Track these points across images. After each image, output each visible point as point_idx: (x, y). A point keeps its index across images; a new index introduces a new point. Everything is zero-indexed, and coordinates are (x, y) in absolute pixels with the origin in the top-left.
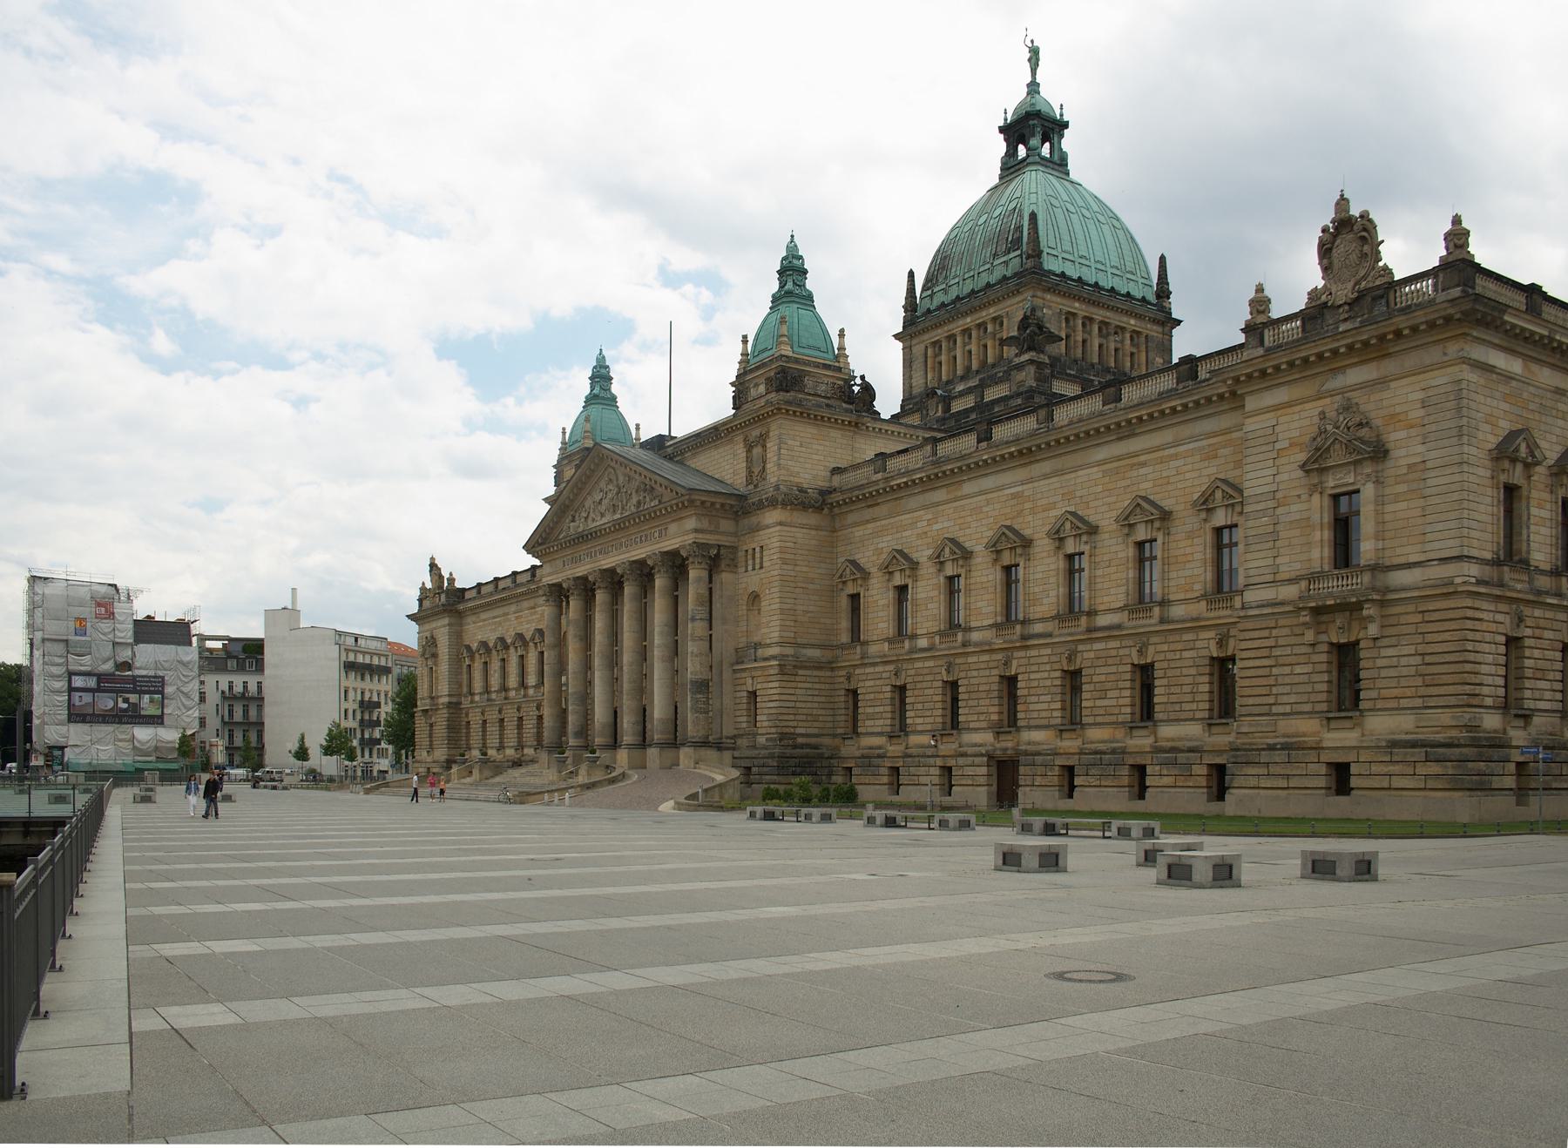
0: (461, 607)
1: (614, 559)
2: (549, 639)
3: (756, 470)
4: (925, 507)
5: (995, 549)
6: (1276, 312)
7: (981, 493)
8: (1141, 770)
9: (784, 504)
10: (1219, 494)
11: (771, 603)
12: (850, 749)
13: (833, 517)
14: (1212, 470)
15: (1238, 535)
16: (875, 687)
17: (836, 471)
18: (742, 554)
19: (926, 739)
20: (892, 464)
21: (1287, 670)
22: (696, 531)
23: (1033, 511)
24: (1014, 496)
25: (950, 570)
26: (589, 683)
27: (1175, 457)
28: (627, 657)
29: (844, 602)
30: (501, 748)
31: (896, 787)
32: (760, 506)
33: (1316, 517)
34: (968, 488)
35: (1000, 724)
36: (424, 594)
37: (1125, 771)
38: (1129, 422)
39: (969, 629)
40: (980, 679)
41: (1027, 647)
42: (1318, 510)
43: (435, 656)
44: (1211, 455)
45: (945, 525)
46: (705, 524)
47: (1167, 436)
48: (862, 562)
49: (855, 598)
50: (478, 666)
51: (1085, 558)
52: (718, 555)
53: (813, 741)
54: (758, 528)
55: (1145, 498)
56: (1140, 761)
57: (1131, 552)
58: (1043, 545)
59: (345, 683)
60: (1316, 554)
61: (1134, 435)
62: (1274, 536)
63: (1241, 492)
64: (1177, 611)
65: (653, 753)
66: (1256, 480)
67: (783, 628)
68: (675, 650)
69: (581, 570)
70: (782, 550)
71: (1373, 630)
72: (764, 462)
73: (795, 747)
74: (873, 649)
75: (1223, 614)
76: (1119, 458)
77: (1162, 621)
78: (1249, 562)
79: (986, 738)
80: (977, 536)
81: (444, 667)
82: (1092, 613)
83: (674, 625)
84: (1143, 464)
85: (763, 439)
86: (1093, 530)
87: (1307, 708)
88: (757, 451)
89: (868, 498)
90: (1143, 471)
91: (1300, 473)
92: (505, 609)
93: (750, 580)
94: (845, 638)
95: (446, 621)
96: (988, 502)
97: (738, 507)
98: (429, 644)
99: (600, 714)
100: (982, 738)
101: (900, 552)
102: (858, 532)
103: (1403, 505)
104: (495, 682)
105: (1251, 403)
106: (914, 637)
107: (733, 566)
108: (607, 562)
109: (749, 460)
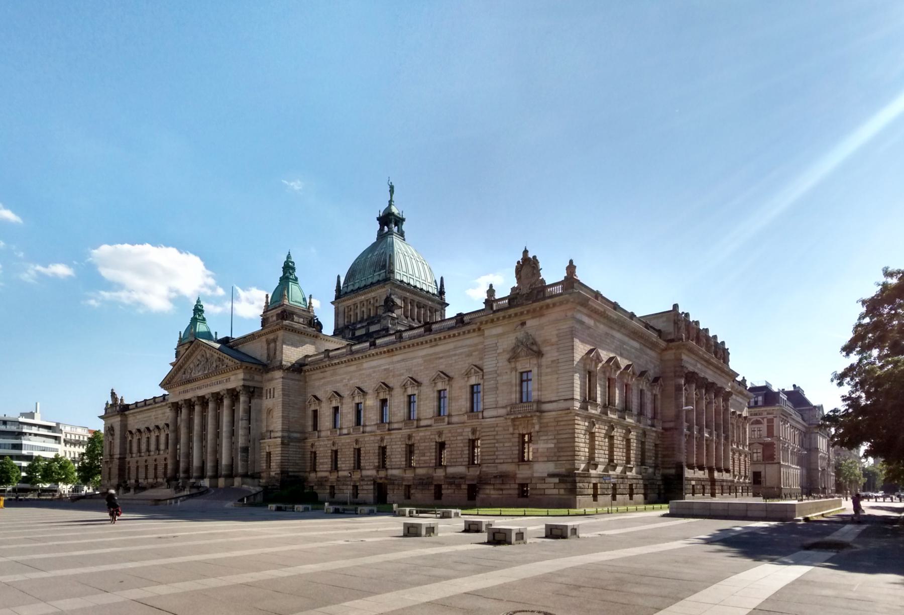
3: (272, 354)
4: (346, 373)
5: (377, 391)
6: (497, 296)
7: (372, 368)
8: (439, 488)
10: (473, 371)
14: (471, 360)
15: (481, 388)
18: (264, 391)
19: (346, 473)
21: (501, 445)
22: (244, 380)
23: (394, 376)
24: (385, 370)
25: (357, 400)
26: (190, 448)
27: (455, 355)
28: (210, 436)
29: (310, 413)
32: (273, 369)
33: (514, 382)
34: (365, 365)
35: (379, 467)
37: (432, 487)
38: (435, 340)
39: (365, 426)
41: (390, 434)
42: (514, 378)
44: (469, 355)
45: (356, 382)
46: (248, 377)
47: (451, 346)
48: (319, 396)
49: (315, 412)
51: (416, 397)
52: (253, 392)
54: (272, 379)
55: (442, 372)
56: (439, 483)
57: (436, 394)
58: (397, 391)
60: (513, 396)
61: (437, 345)
62: (497, 388)
63: (482, 370)
64: (454, 419)
66: (489, 365)
68: (232, 433)
70: (283, 390)
71: (537, 428)
72: (275, 350)
74: (323, 434)
75: (475, 422)
76: (431, 355)
77: (449, 423)
78: (487, 400)
79: (372, 473)
80: (369, 386)
82: (419, 420)
83: (232, 422)
84: (441, 358)
85: (275, 340)
86: (419, 384)
87: (510, 460)
88: (272, 345)
90: (441, 361)
91: (507, 363)
93: (267, 403)
94: (310, 429)
96: (374, 372)
99: (196, 462)
100: (371, 473)
101: (336, 392)
102: (317, 383)
103: (549, 377)
105: (487, 333)
106: (341, 429)
107: (260, 396)
108: (201, 393)
109: (268, 349)
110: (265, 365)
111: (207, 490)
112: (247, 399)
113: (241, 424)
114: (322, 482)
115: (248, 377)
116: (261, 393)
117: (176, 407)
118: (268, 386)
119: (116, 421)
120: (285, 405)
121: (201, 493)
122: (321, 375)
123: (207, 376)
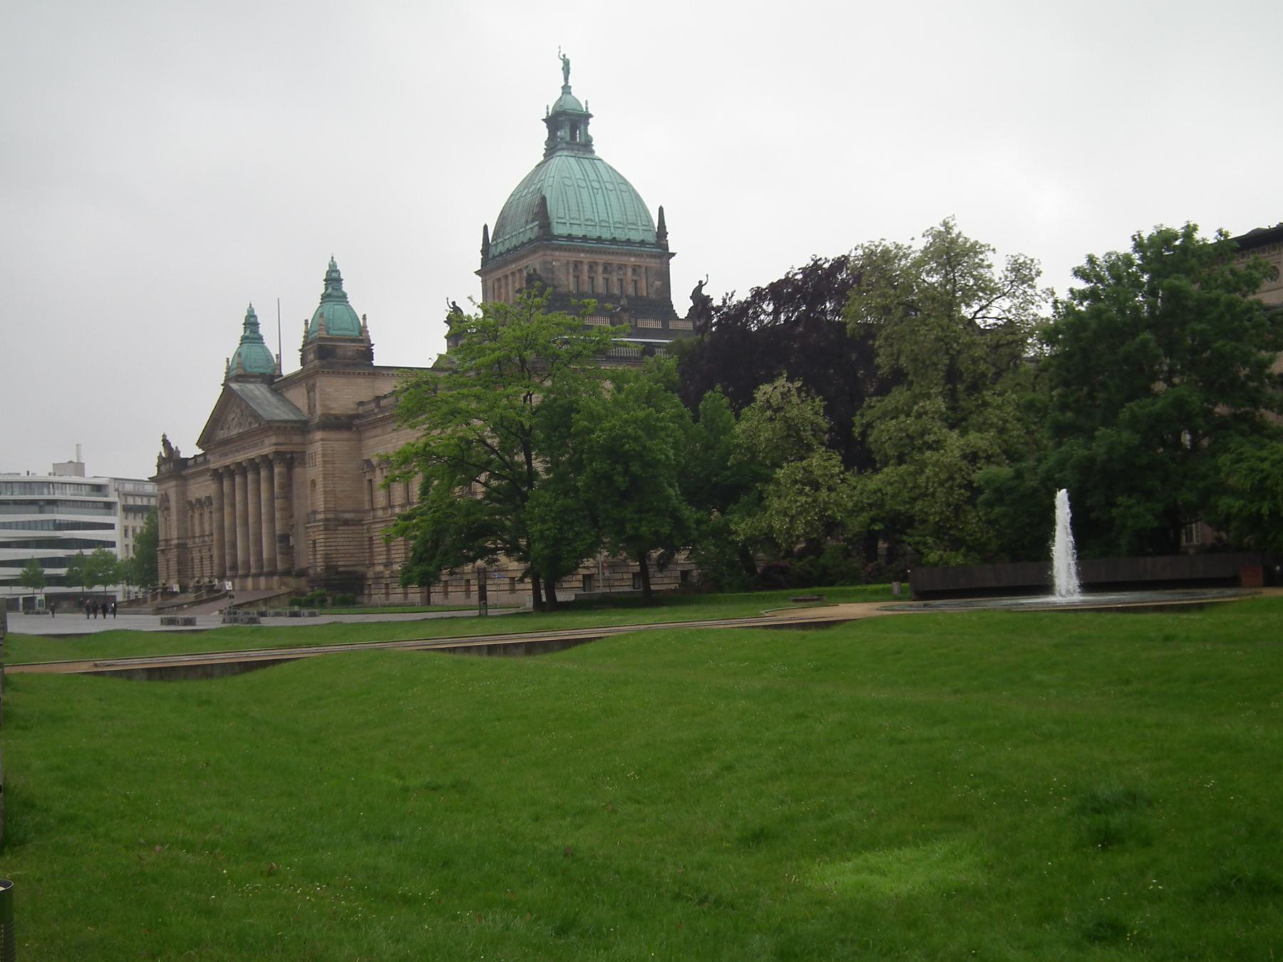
0: (184, 473)
1: (240, 457)
2: (215, 505)
11: (320, 488)
12: (370, 574)
13: (359, 432)
17: (361, 404)
20: (383, 403)
22: (276, 444)
29: (366, 484)
31: (387, 594)
36: (162, 461)
43: (167, 509)
46: (282, 439)
49: (370, 481)
50: (197, 516)
52: (292, 458)
53: (350, 569)
59: (126, 523)
69: (228, 461)
70: (324, 455)
73: (338, 573)
85: (314, 385)
89: (373, 425)
94: (367, 507)
95: (173, 483)
97: (302, 427)
98: (165, 498)
102: (371, 442)
106: (392, 507)
107: (303, 463)
110: (305, 423)
112: (284, 470)
113: (278, 503)
114: (379, 577)
115: (282, 439)
116: (303, 460)
117: (218, 475)
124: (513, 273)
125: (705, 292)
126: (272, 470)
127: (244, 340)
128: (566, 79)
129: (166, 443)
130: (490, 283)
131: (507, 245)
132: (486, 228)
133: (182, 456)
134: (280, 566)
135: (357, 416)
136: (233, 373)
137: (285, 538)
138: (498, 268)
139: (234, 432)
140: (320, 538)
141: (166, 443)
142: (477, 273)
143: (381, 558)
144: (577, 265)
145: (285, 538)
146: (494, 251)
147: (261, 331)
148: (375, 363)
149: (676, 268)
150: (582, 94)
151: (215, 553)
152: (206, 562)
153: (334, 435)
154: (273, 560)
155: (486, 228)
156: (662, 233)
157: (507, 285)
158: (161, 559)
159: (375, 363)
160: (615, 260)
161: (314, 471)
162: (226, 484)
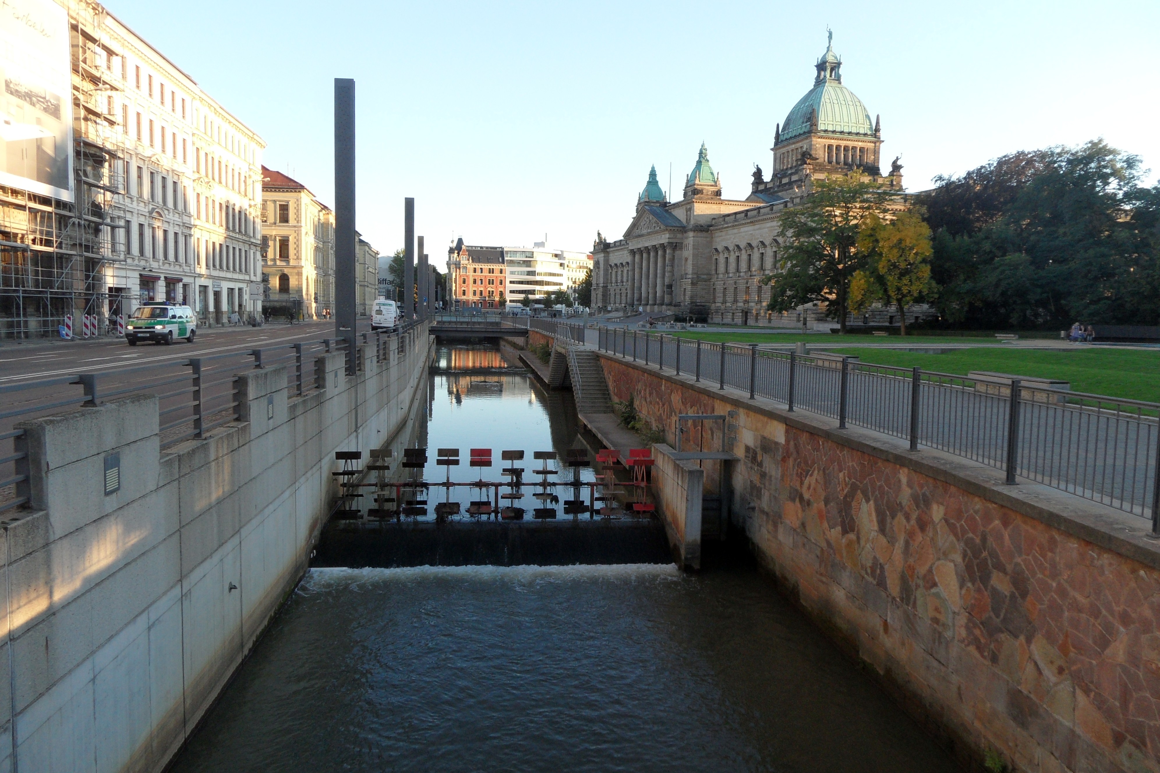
9: (694, 231)
11: (690, 262)
12: (713, 307)
16: (719, 287)
20: (727, 219)
29: (714, 261)
30: (621, 303)
34: (742, 230)
40: (742, 287)
43: (598, 268)
46: (672, 236)
54: (687, 238)
65: (656, 307)
67: (693, 269)
81: (602, 272)
92: (621, 253)
94: (713, 272)
102: (718, 240)
104: (619, 278)
107: (681, 249)
110: (684, 227)
111: (640, 314)
113: (668, 269)
115: (672, 236)
117: (633, 252)
118: (686, 242)
119: (601, 256)
120: (694, 255)
121: (636, 315)
122: (720, 234)
123: (649, 234)
124: (792, 150)
125: (899, 163)
126: (665, 251)
127: (649, 182)
128: (830, 42)
129: (599, 234)
130: (778, 155)
131: (790, 135)
132: (778, 125)
133: (608, 241)
134: (666, 300)
135: (711, 226)
136: (642, 201)
137: (670, 286)
138: (784, 147)
139: (644, 231)
140: (689, 288)
141: (599, 234)
142: (772, 149)
143: (719, 300)
144: (830, 147)
145: (670, 286)
146: (781, 138)
147: (658, 179)
148: (722, 198)
149: (883, 148)
150: (839, 51)
151: (629, 292)
152: (618, 296)
153: (700, 234)
154: (663, 297)
155: (778, 125)
156: (877, 130)
157: (788, 156)
158: (593, 293)
159: (722, 198)
160: (850, 144)
161: (688, 253)
162: (637, 257)
